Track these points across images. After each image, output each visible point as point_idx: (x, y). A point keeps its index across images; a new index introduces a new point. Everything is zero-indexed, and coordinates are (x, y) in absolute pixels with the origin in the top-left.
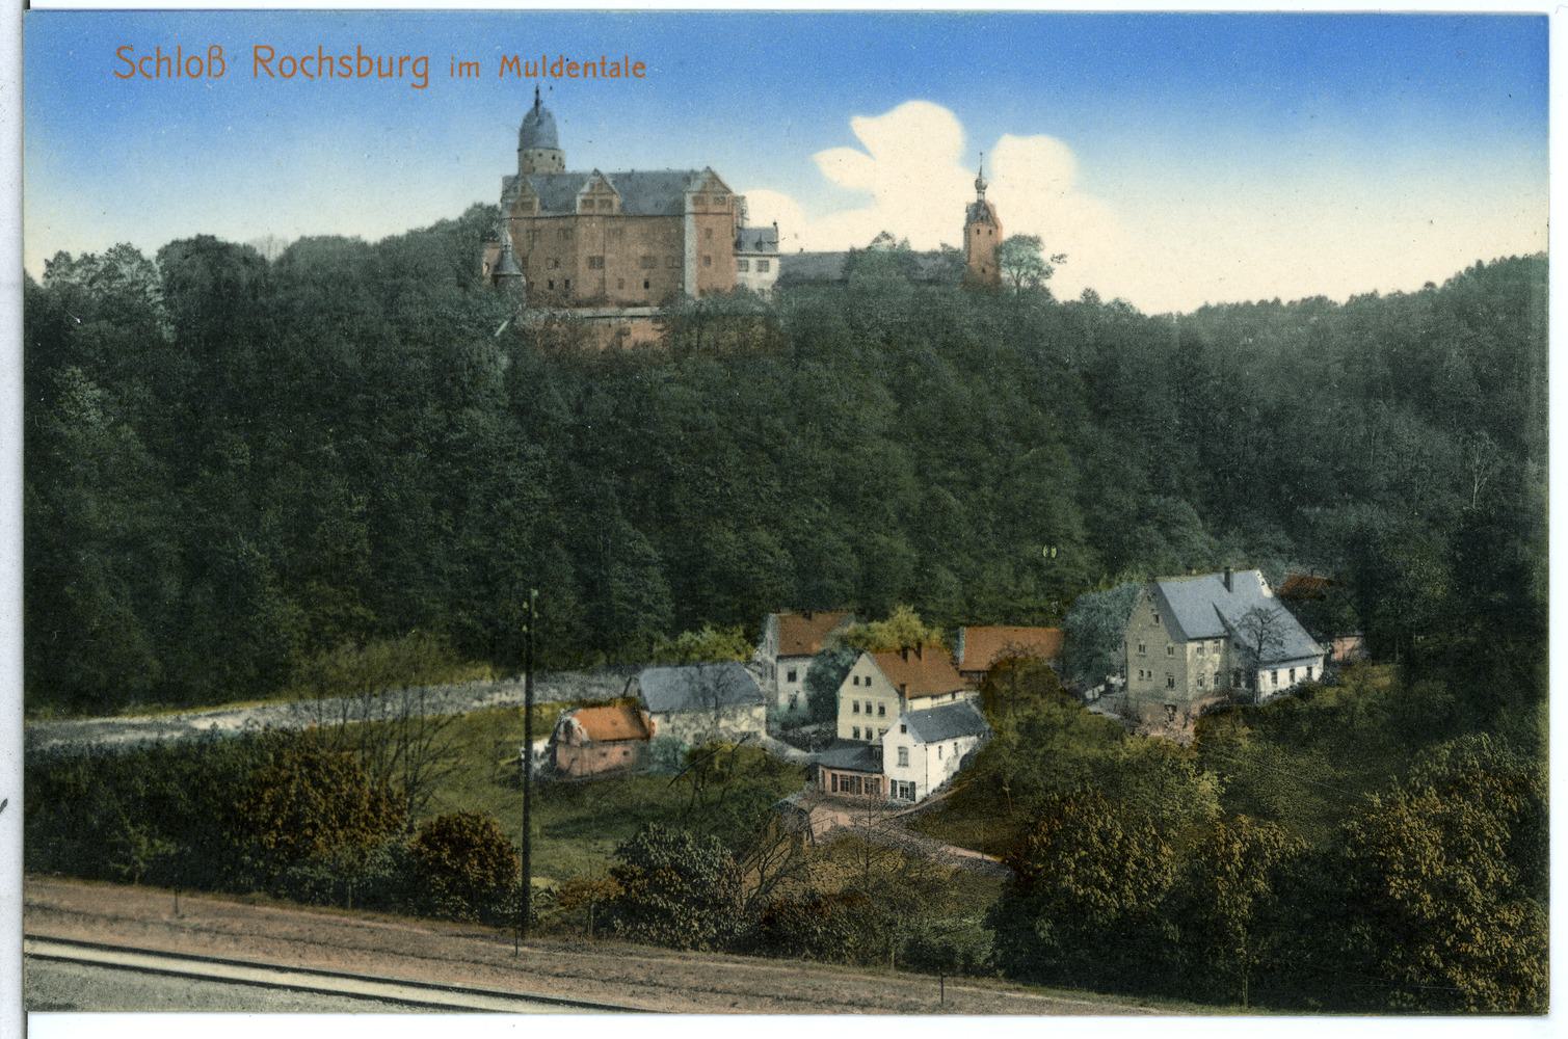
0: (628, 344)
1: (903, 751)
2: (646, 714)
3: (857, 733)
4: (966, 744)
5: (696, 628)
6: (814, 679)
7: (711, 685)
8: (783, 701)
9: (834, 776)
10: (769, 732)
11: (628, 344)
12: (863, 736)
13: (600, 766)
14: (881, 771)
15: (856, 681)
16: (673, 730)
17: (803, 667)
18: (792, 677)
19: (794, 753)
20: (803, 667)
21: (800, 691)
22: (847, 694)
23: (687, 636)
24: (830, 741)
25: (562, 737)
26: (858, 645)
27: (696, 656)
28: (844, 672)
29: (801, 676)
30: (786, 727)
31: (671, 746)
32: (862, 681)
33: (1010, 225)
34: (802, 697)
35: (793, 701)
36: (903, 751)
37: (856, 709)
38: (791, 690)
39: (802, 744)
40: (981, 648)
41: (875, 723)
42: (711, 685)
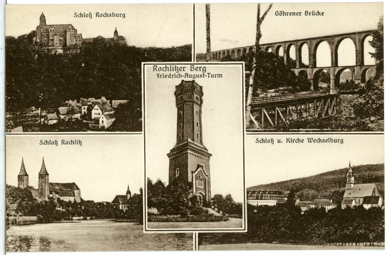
0: (57, 54)
1: (103, 121)
2: (60, 115)
3: (95, 118)
4: (113, 120)
5: (68, 100)
6: (88, 109)
7: (71, 110)
8: (83, 113)
9: (91, 125)
10: (81, 118)
11: (57, 54)
12: (96, 119)
13: (52, 123)
14: (99, 124)
15: (95, 109)
16: (65, 117)
17: (86, 107)
18: (84, 108)
19: (84, 121)
20: (86, 107)
21: (86, 110)
22: (93, 112)
23: (67, 102)
24: (90, 119)
25: (46, 119)
26: (95, 104)
27: (68, 105)
28: (93, 108)
29: (86, 108)
30: (83, 117)
31: (63, 120)
32: (96, 109)
33: (120, 34)
34: (86, 112)
35: (84, 112)
36: (103, 121)
37: (95, 114)
38: (84, 110)
39: (86, 120)
40: (116, 103)
41: (98, 116)
42: (71, 110)
